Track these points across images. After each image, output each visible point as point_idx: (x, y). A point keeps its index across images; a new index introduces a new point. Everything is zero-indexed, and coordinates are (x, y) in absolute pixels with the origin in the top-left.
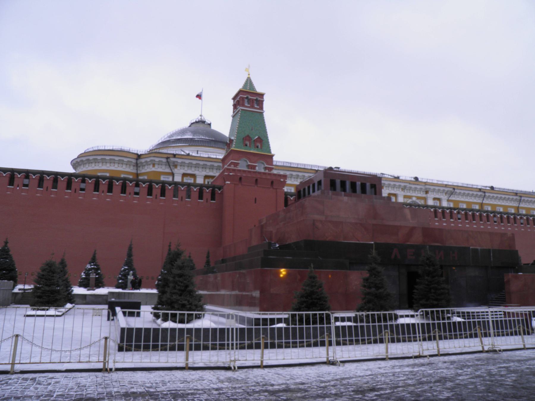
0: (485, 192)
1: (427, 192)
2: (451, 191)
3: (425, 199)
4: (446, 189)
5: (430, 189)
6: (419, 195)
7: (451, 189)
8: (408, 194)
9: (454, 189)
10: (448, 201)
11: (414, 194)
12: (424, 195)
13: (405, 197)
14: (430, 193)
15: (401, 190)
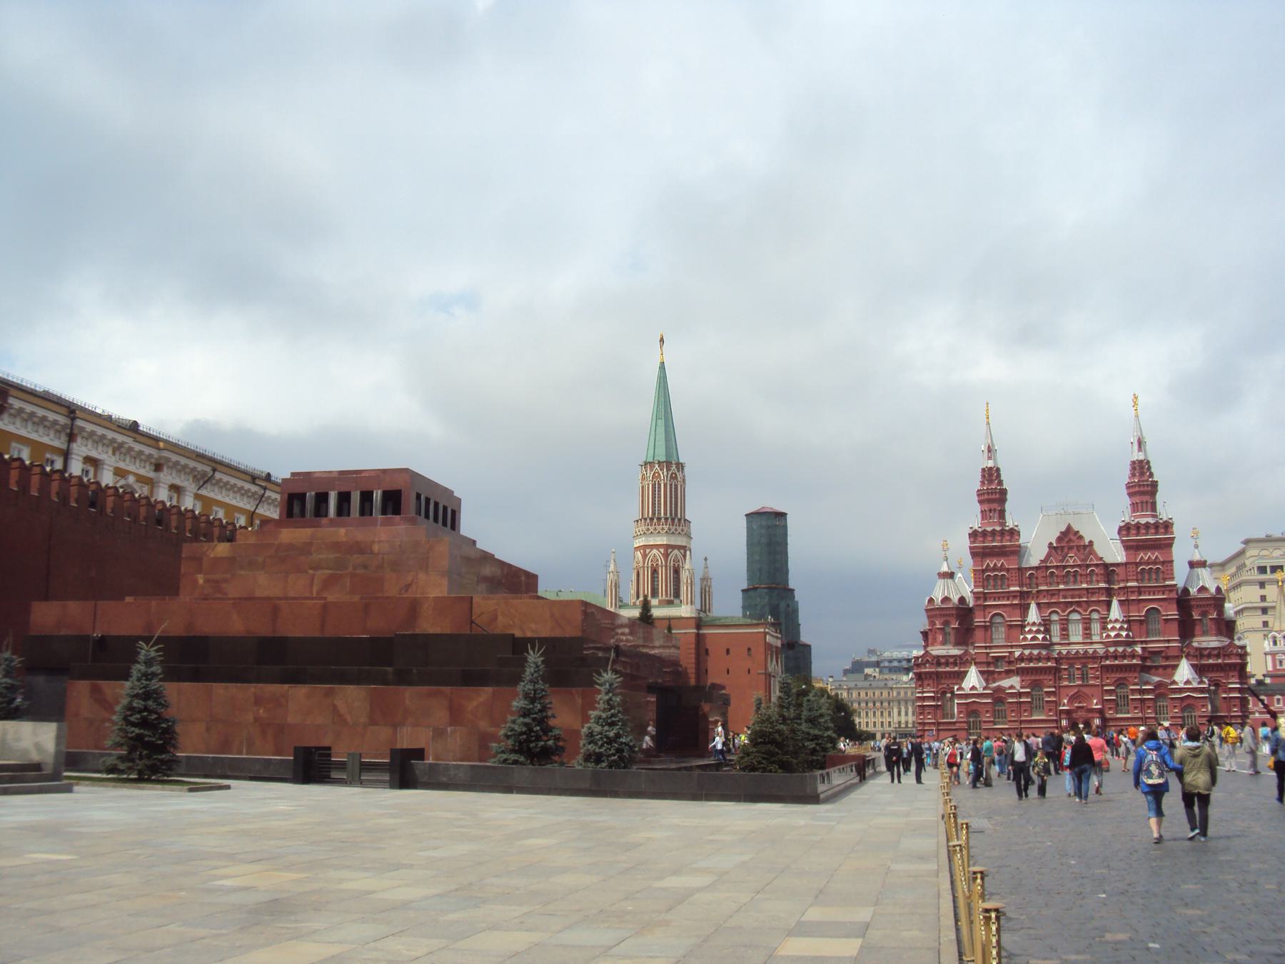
0: (265, 489)
1: (158, 467)
2: (204, 474)
3: (151, 483)
4: (200, 467)
5: (168, 460)
6: (142, 472)
7: (208, 469)
8: (122, 465)
9: (214, 470)
10: (197, 497)
11: (132, 468)
12: (152, 475)
13: (119, 473)
14: (165, 469)
15: (110, 452)
